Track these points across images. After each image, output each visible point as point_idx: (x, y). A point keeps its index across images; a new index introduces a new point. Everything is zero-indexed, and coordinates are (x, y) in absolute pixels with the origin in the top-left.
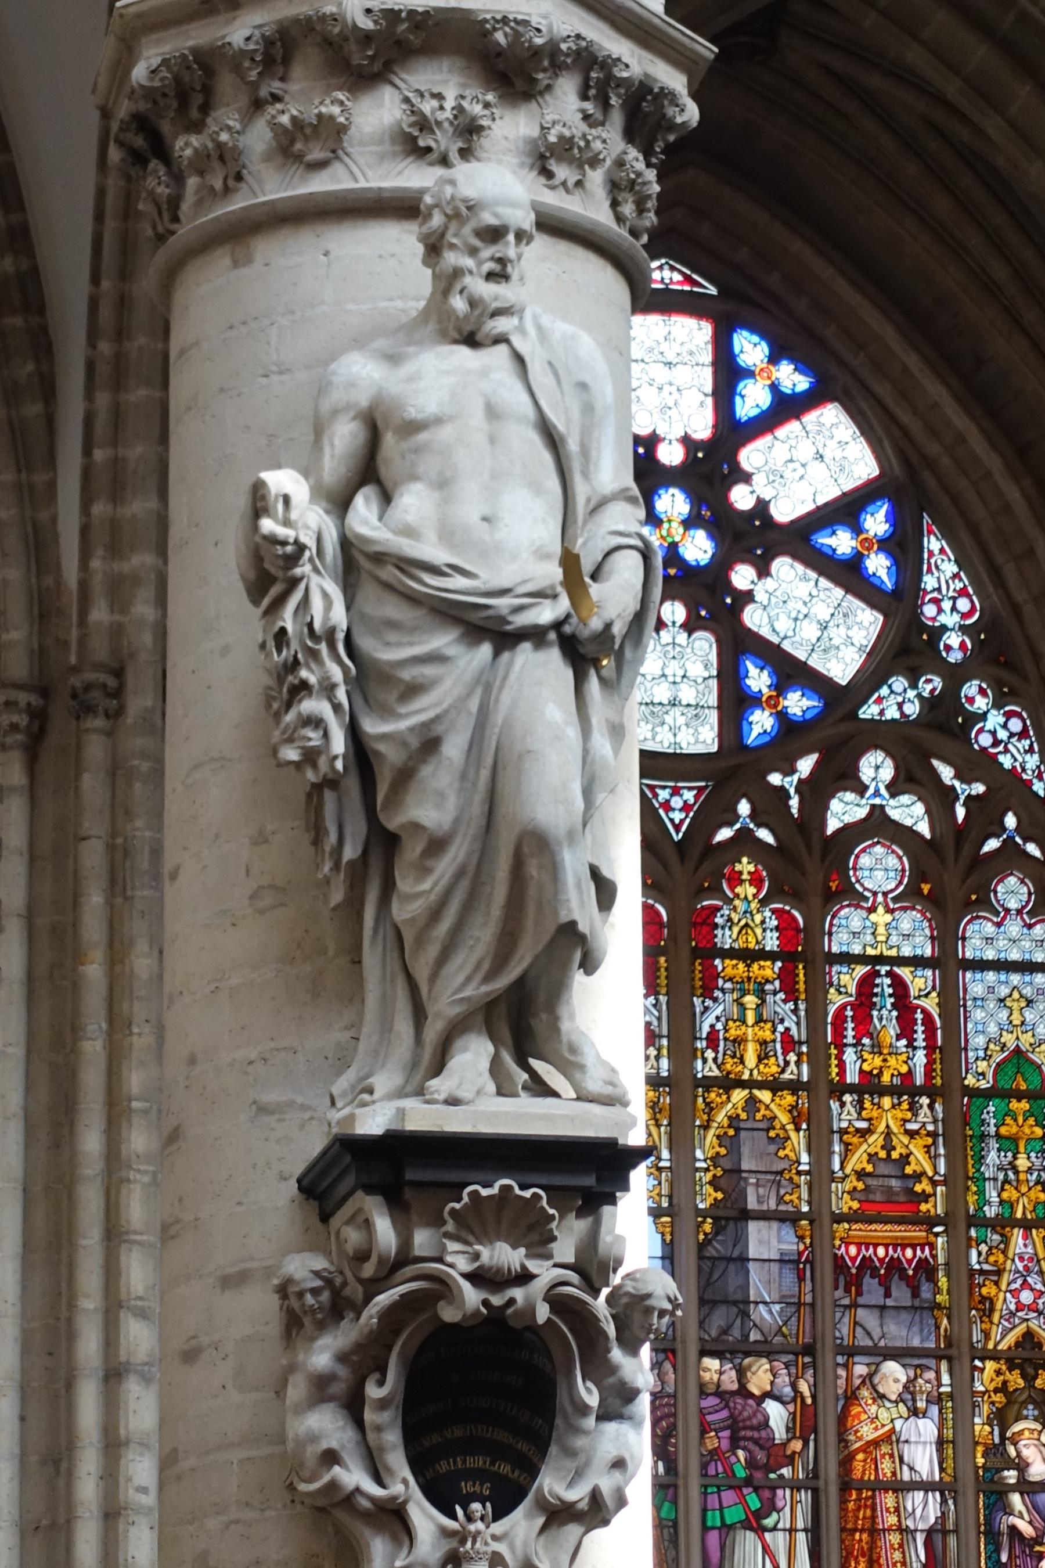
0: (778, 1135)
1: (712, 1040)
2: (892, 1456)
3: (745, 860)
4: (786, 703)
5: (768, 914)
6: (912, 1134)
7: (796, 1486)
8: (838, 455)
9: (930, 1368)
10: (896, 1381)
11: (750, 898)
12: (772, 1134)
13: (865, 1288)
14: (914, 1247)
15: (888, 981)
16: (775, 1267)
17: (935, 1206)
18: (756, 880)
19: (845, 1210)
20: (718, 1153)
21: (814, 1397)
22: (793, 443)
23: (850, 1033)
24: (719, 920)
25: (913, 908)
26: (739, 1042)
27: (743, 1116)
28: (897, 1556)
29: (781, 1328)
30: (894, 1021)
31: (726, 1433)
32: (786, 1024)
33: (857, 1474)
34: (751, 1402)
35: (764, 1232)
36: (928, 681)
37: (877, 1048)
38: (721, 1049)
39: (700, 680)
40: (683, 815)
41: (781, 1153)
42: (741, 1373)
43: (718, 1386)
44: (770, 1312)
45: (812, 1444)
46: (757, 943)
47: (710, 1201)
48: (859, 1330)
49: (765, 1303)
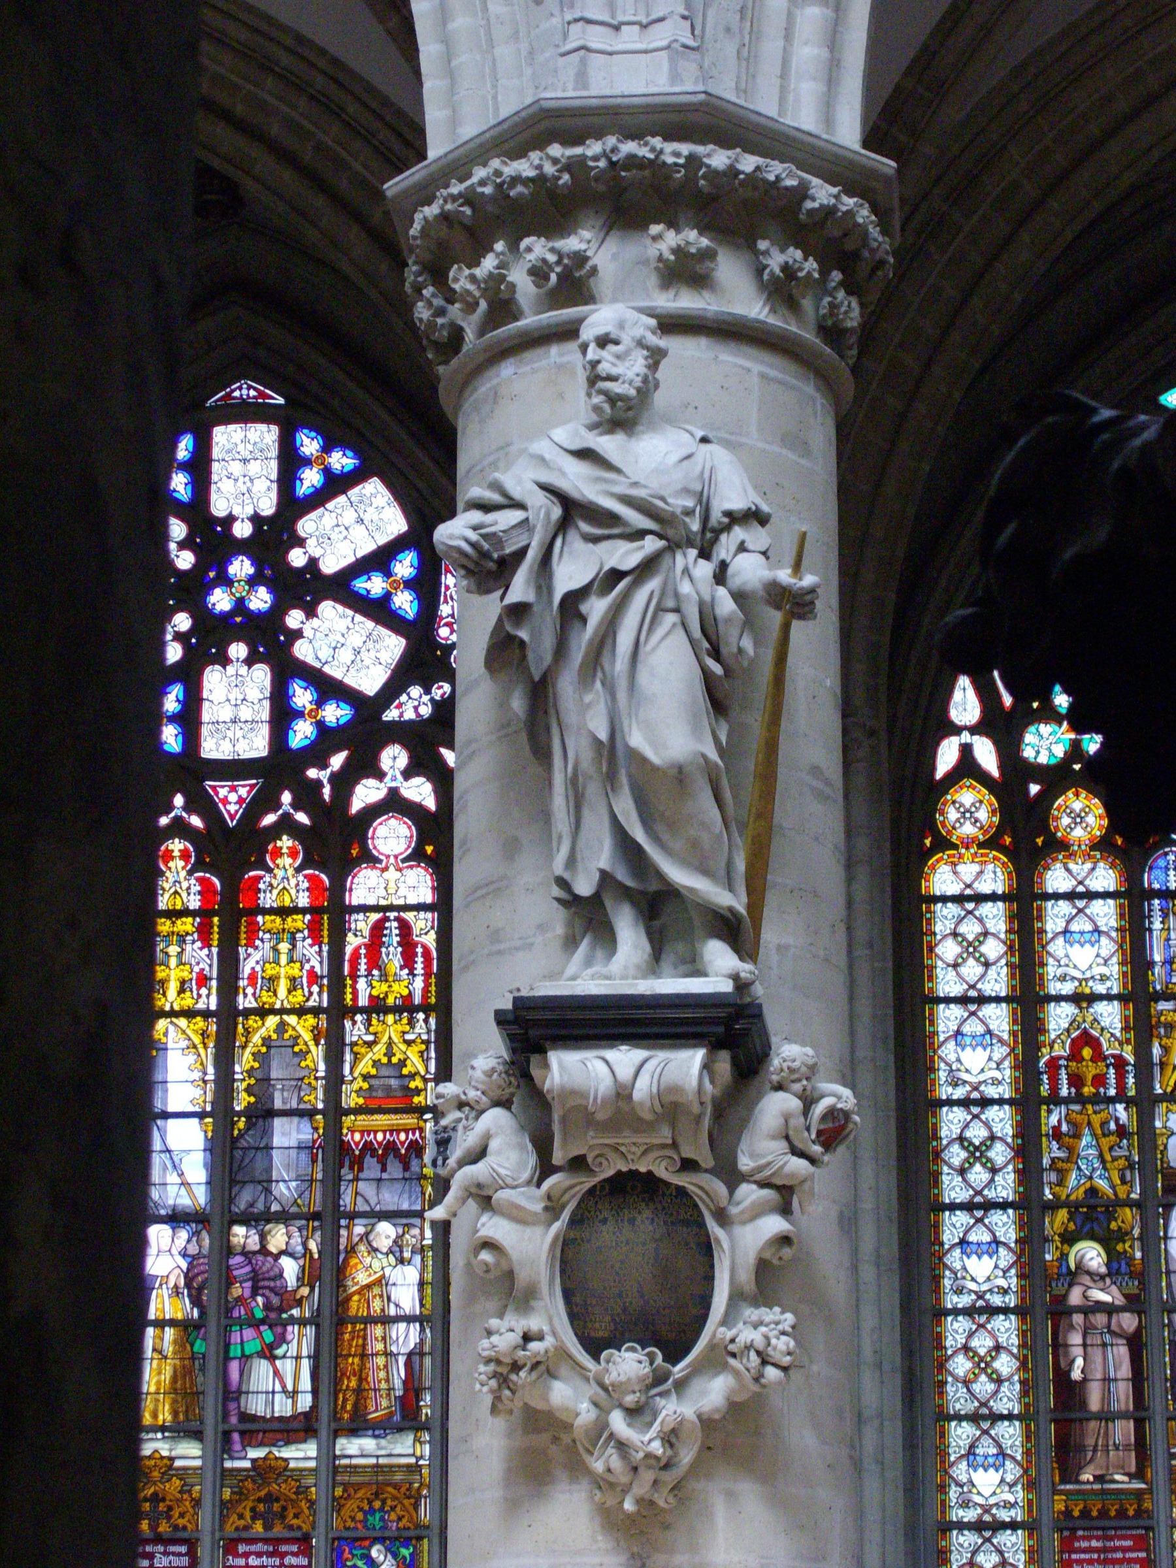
0: (301, 1050)
1: (253, 978)
2: (381, 1296)
3: (285, 837)
4: (324, 713)
5: (301, 878)
6: (409, 1043)
7: (302, 1322)
8: (375, 518)
9: (414, 1226)
10: (388, 1237)
11: (287, 867)
12: (297, 1049)
13: (365, 1166)
14: (407, 1131)
15: (395, 924)
16: (293, 1153)
17: (426, 1099)
18: (293, 854)
19: (353, 1105)
20: (252, 1067)
21: (320, 1252)
22: (339, 511)
23: (363, 967)
24: (261, 886)
25: (419, 866)
26: (273, 980)
27: (274, 1036)
28: (382, 1374)
29: (296, 1201)
30: (399, 955)
31: (248, 1284)
32: (312, 963)
33: (352, 1312)
34: (270, 1259)
35: (287, 1126)
36: (440, 687)
37: (384, 977)
38: (259, 986)
39: (256, 701)
40: (237, 807)
41: (303, 1064)
42: (263, 1237)
43: (244, 1247)
44: (289, 1188)
45: (317, 1290)
46: (292, 901)
47: (244, 1104)
48: (359, 1199)
49: (285, 1181)
